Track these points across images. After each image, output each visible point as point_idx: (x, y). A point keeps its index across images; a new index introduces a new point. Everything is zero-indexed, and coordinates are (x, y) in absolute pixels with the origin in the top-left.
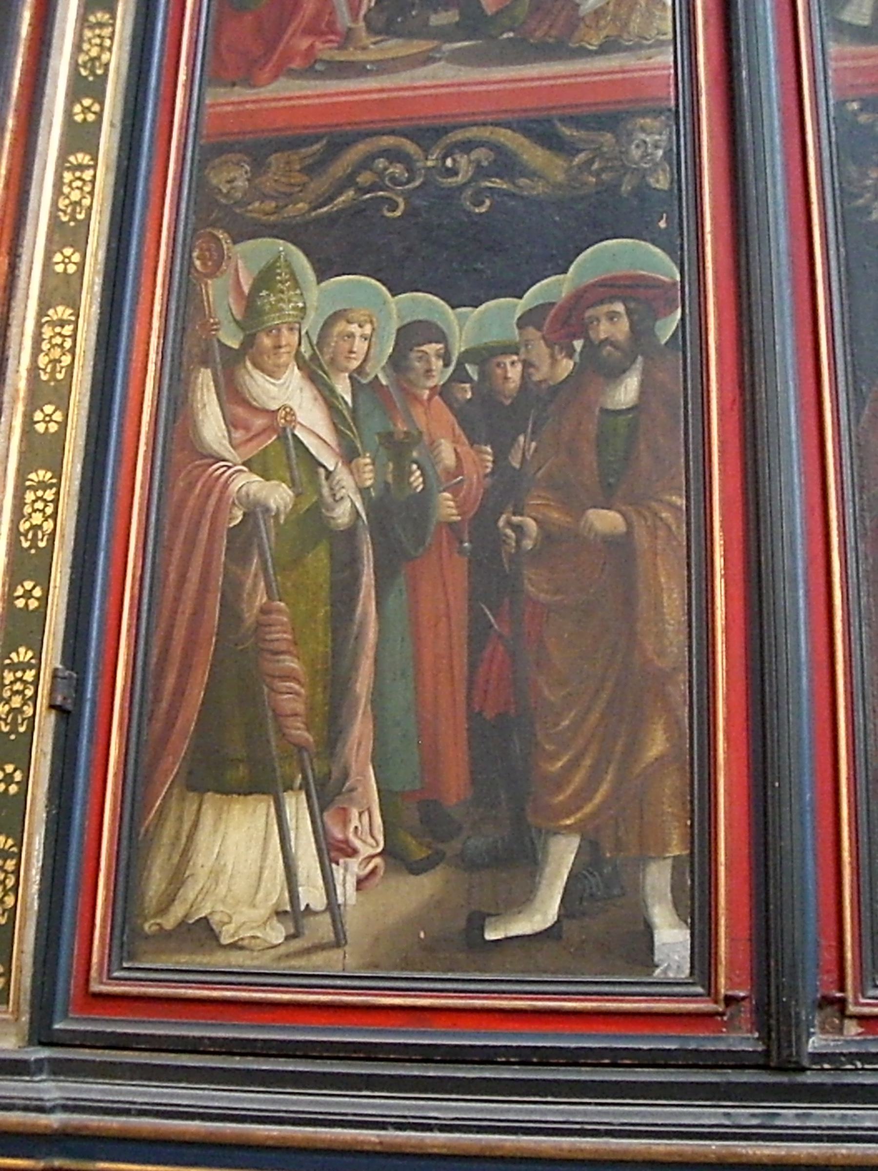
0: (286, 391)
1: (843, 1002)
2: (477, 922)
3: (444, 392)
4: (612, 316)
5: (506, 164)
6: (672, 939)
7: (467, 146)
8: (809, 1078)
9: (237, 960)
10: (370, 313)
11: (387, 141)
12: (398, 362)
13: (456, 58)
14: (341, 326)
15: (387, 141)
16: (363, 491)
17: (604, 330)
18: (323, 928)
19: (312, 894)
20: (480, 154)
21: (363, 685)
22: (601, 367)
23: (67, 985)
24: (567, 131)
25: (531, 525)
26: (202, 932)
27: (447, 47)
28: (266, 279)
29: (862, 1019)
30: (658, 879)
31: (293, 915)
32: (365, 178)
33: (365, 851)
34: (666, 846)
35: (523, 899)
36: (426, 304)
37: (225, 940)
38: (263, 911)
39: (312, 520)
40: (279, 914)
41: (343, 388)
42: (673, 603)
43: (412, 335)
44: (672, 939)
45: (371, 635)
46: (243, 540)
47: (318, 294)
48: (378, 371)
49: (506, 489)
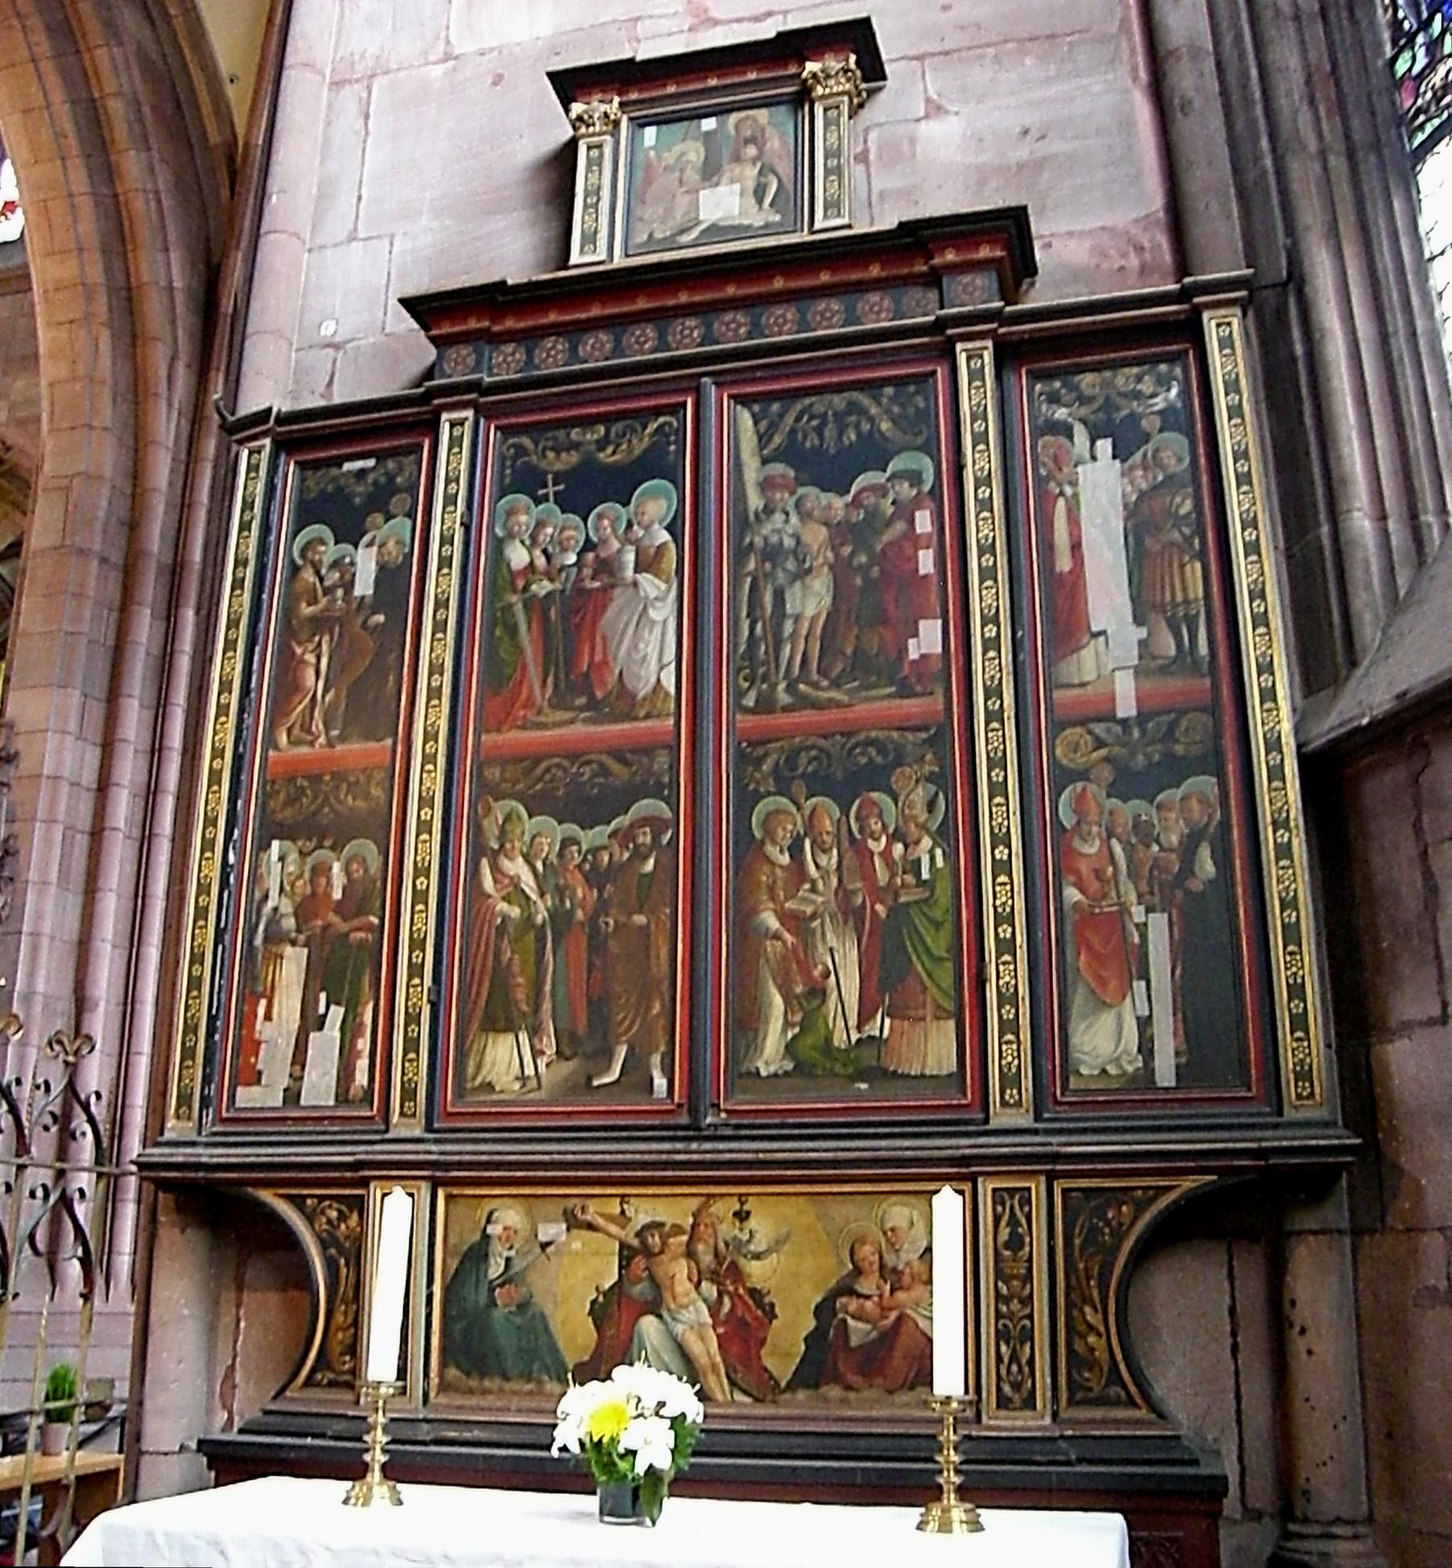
0: (517, 867)
1: (718, 1105)
2: (590, 1079)
3: (579, 867)
4: (645, 834)
5: (605, 771)
6: (660, 1082)
7: (588, 763)
8: (706, 1133)
9: (502, 1097)
10: (549, 832)
11: (557, 760)
12: (561, 855)
13: (584, 721)
14: (538, 840)
15: (557, 760)
16: (548, 910)
17: (641, 840)
18: (534, 1083)
19: (529, 1071)
20: (594, 766)
21: (548, 988)
22: (640, 855)
23: (438, 1109)
24: (628, 755)
25: (612, 922)
26: (489, 1087)
27: (582, 716)
28: (508, 818)
29: (727, 1111)
30: (656, 1059)
31: (523, 1078)
32: (548, 777)
33: (549, 1053)
34: (657, 1048)
35: (608, 1068)
36: (573, 829)
37: (498, 1089)
38: (511, 1077)
39: (528, 920)
40: (517, 1078)
41: (539, 866)
42: (664, 952)
43: (566, 843)
44: (660, 1082)
45: (551, 970)
46: (501, 930)
47: (529, 825)
48: (553, 858)
49: (602, 907)
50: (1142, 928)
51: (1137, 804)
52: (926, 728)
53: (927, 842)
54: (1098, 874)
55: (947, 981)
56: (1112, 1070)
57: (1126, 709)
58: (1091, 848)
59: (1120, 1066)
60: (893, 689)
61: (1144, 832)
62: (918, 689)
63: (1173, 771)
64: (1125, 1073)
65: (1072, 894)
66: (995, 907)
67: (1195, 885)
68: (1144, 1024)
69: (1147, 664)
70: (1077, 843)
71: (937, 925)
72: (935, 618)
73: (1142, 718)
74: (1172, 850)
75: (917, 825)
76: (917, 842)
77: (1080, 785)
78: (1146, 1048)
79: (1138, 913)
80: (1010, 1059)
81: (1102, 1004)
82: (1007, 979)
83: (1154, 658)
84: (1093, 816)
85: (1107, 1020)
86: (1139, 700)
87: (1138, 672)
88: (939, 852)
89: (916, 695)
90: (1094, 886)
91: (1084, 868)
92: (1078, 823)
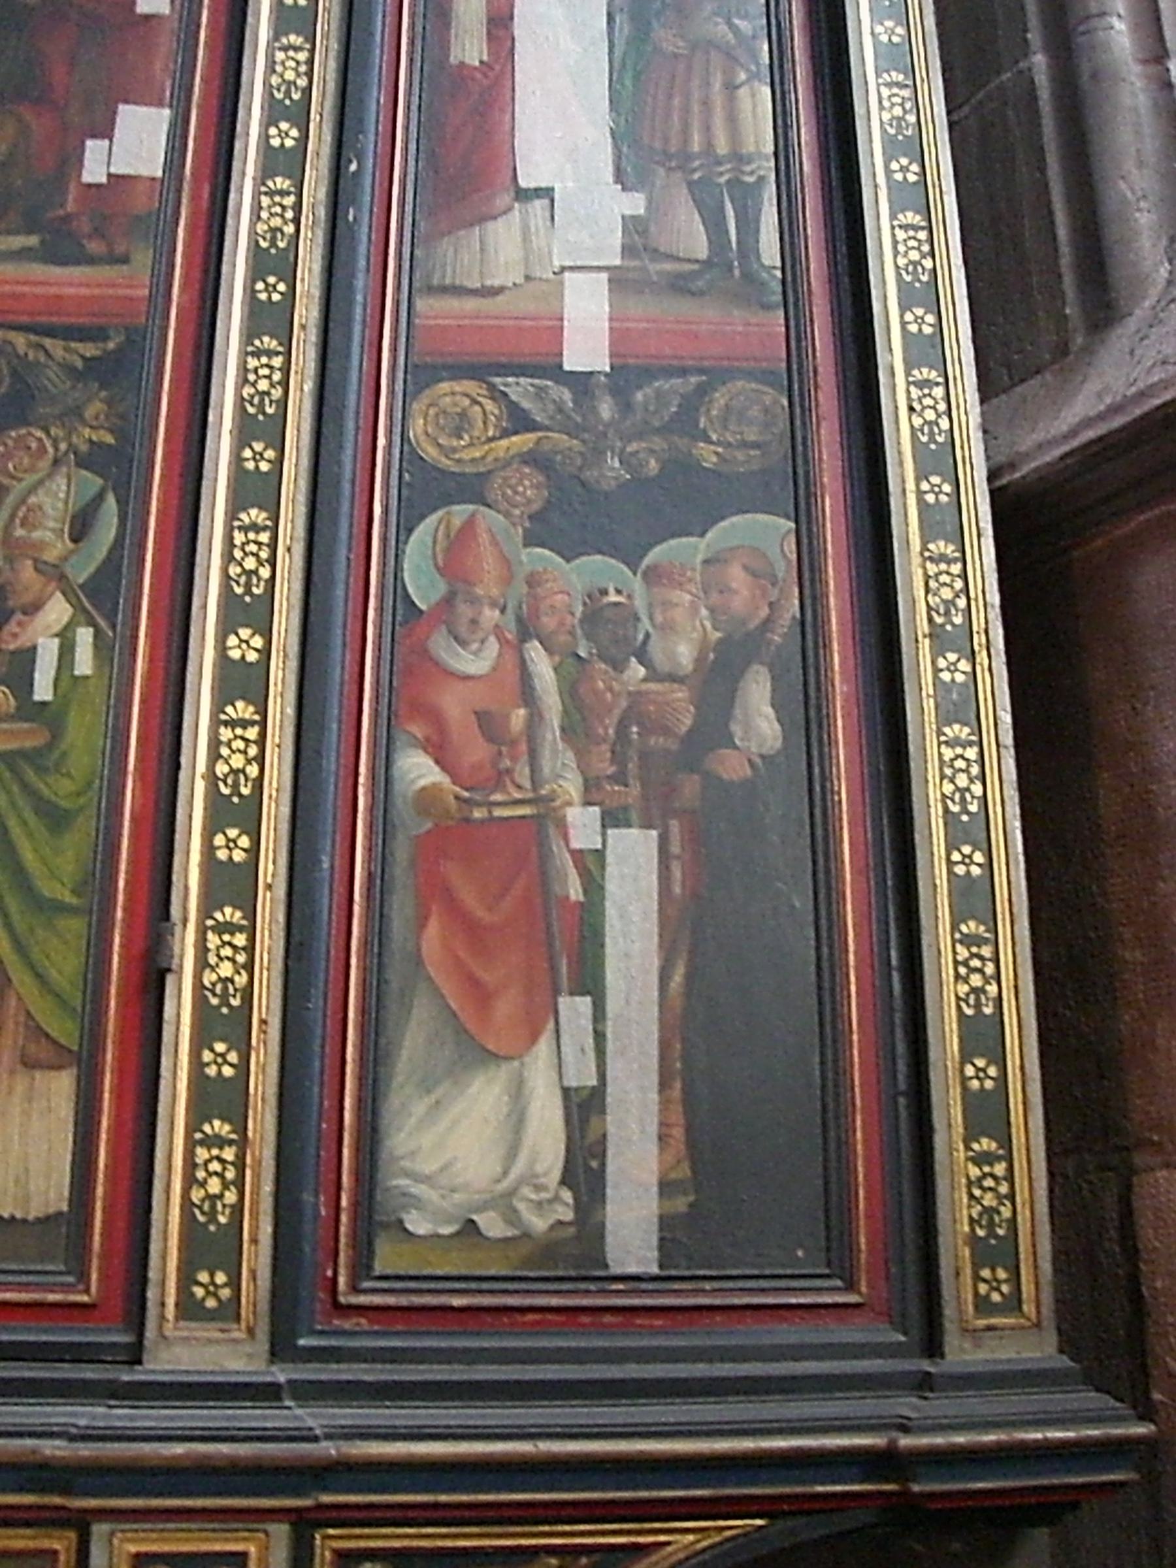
50: (591, 865)
51: (598, 568)
52: (96, 334)
53: (58, 611)
54: (488, 723)
55: (65, 963)
56: (492, 1225)
57: (586, 349)
58: (476, 661)
59: (511, 1216)
60: (33, 240)
61: (609, 630)
62: (94, 247)
63: (690, 497)
64: (526, 1235)
65: (418, 769)
66: (212, 779)
67: (732, 767)
68: (584, 1108)
69: (640, 267)
70: (441, 646)
71: (56, 819)
72: (160, 104)
73: (625, 375)
74: (673, 678)
75: (39, 566)
76: (34, 608)
77: (460, 512)
78: (585, 1170)
79: (583, 825)
80: (214, 1186)
81: (472, 1051)
82: (226, 970)
83: (656, 254)
84: (488, 586)
85: (485, 1094)
86: (619, 337)
87: (619, 281)
88: (84, 636)
89: (91, 261)
90: (476, 751)
91: (454, 705)
92: (448, 601)
